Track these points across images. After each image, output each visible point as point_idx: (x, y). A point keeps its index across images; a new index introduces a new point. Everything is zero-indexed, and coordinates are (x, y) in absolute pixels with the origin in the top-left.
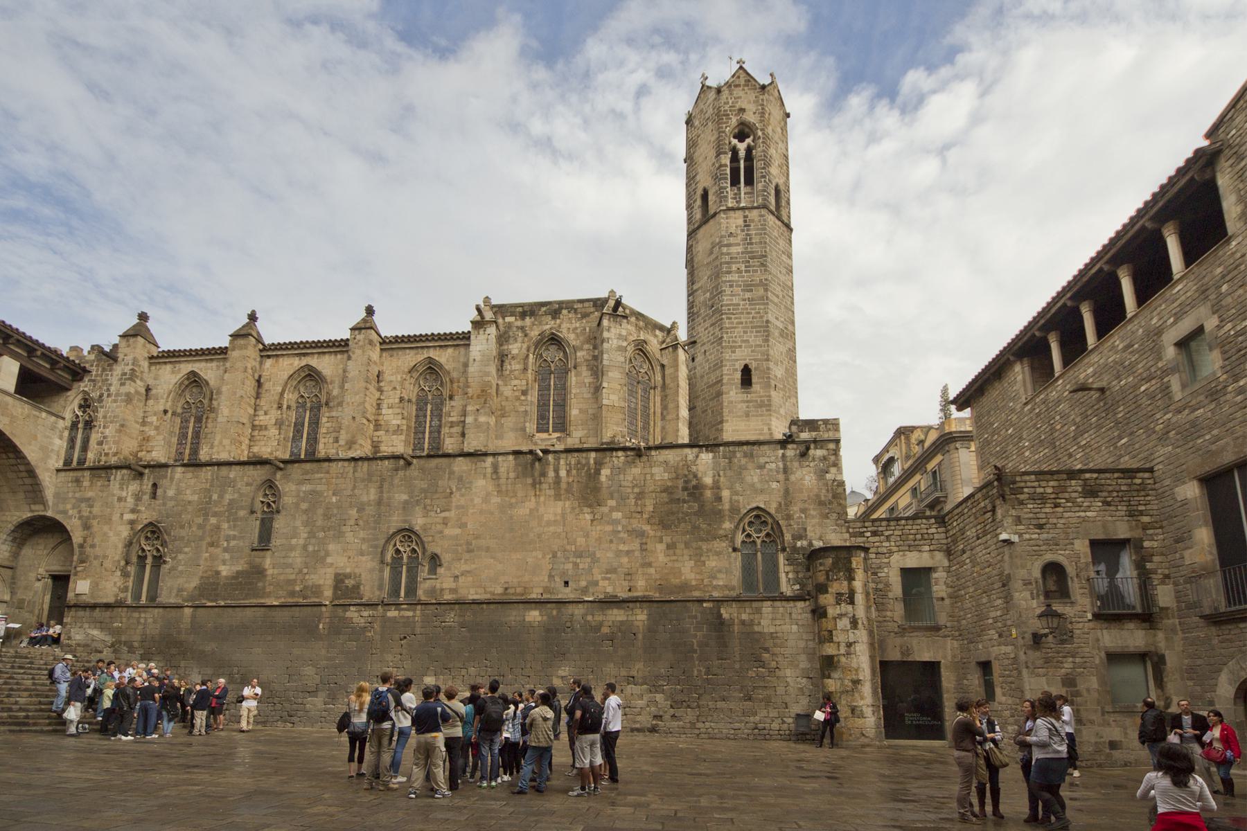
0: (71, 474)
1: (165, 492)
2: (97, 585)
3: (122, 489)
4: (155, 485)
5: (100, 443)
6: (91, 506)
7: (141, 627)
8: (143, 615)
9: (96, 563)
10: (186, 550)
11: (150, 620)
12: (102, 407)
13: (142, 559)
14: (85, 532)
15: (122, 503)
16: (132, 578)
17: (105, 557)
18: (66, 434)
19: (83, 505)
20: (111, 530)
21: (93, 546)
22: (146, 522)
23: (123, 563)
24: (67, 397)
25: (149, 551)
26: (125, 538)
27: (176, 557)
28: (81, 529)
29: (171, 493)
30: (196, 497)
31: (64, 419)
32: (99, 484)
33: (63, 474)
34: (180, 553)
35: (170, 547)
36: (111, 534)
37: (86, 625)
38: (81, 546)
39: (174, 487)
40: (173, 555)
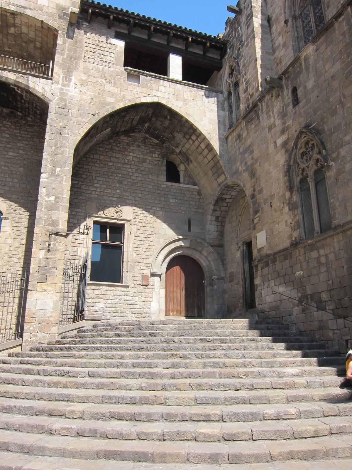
0: (235, 134)
1: (305, 87)
2: (272, 231)
3: (269, 117)
4: (295, 91)
5: (246, 90)
6: (252, 152)
7: (323, 269)
8: (322, 252)
9: (266, 207)
10: (347, 138)
11: (331, 257)
12: (240, 60)
13: (304, 181)
14: (253, 180)
15: (273, 131)
16: (300, 209)
17: (272, 196)
18: (226, 105)
19: (247, 155)
20: (270, 165)
21: (261, 191)
22: (296, 134)
23: (288, 195)
24: (221, 75)
25: (308, 167)
26: (284, 165)
27: (337, 157)
28: (249, 179)
29: (310, 84)
30: (338, 66)
31: (222, 92)
32: (253, 126)
33: (230, 138)
34: (342, 146)
35: (328, 146)
36: (271, 170)
37: (272, 283)
38: (253, 196)
39: (311, 75)
40: (334, 155)
